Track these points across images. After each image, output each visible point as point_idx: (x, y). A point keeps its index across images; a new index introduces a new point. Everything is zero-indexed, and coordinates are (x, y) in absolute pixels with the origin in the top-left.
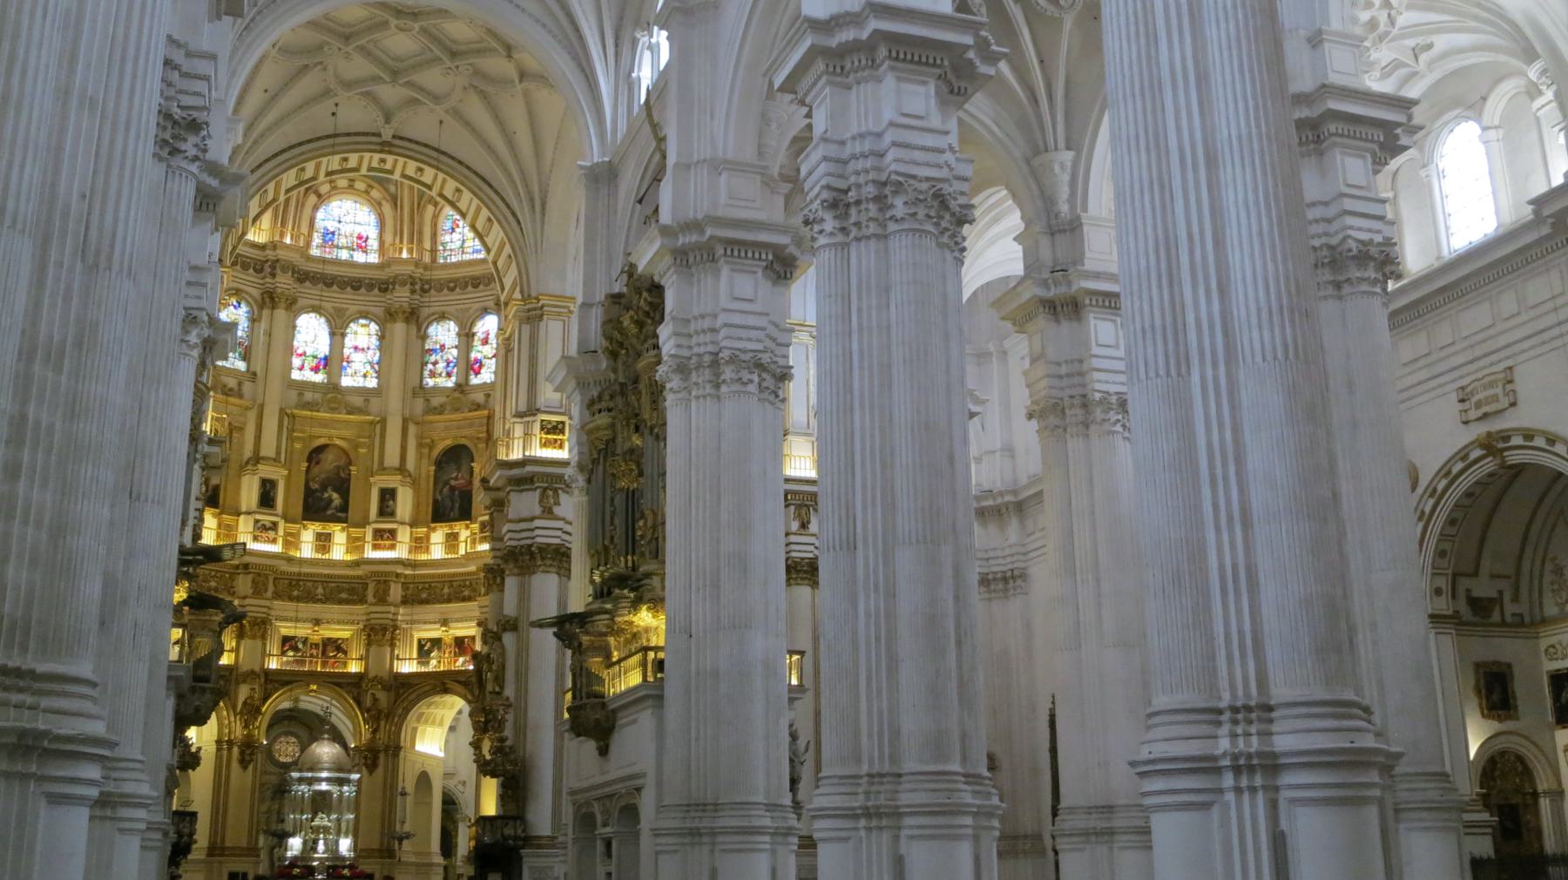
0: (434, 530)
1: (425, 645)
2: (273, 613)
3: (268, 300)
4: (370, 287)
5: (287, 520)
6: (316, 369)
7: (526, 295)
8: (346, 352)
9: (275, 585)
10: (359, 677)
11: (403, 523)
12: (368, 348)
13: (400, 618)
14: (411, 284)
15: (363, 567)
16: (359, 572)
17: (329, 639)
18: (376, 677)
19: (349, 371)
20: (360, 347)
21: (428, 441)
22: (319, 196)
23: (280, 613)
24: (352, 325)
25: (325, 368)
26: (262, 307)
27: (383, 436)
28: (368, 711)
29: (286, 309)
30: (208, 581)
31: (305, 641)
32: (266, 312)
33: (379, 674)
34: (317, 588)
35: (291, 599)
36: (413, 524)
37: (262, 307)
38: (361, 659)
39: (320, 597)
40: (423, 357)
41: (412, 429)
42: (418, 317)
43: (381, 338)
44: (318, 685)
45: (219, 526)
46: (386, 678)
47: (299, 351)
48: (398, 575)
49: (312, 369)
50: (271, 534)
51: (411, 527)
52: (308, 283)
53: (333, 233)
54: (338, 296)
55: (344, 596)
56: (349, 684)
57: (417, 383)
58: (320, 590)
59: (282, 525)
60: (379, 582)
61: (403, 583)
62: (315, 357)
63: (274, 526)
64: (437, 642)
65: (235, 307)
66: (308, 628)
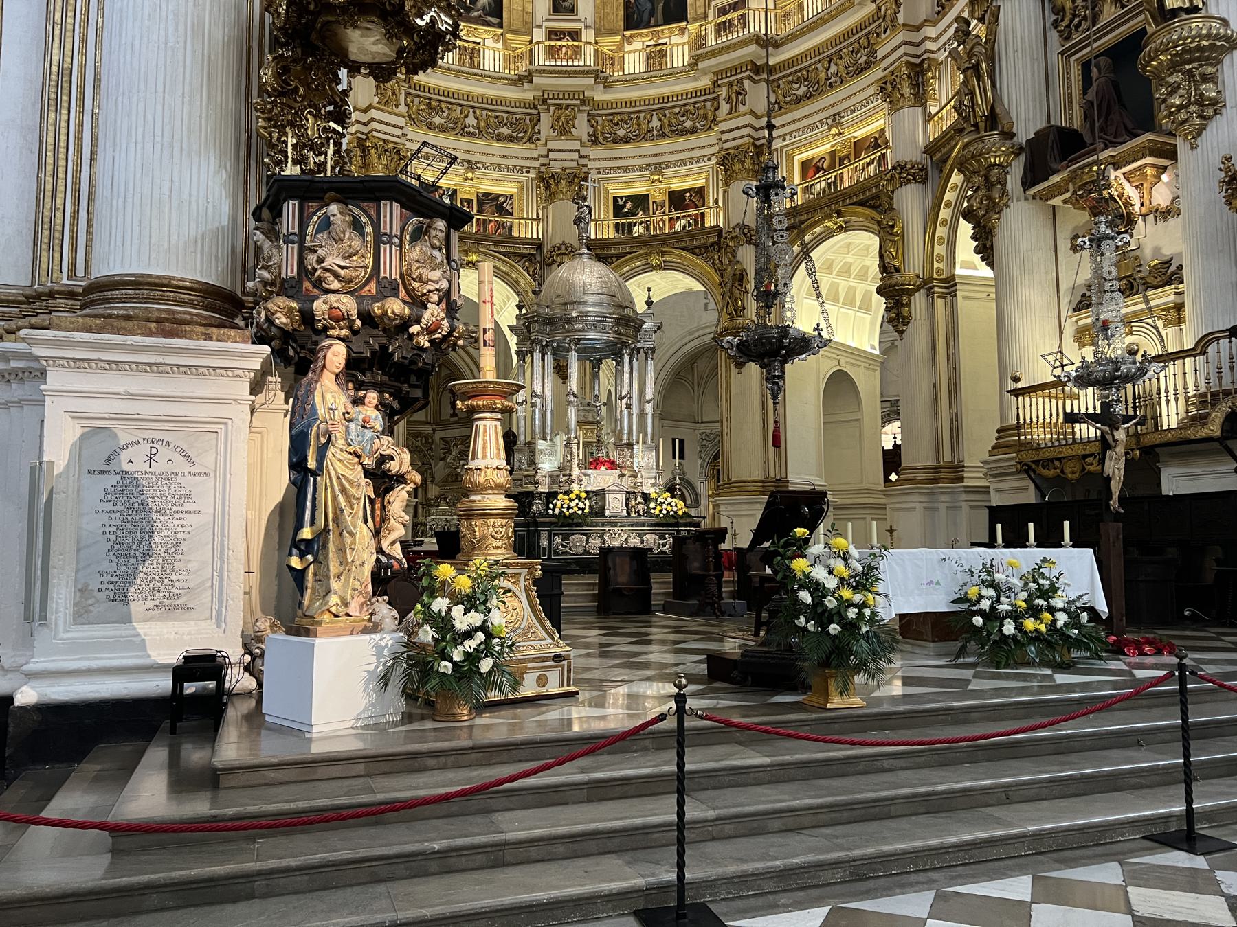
0: (630, 40)
1: (624, 206)
9: (407, 105)
10: (538, 245)
13: (591, 165)
16: (525, 94)
17: (486, 195)
18: (563, 243)
34: (466, 117)
38: (538, 219)
39: (471, 130)
55: (505, 131)
56: (522, 256)
58: (471, 120)
60: (559, 107)
61: (589, 115)
64: (641, 201)
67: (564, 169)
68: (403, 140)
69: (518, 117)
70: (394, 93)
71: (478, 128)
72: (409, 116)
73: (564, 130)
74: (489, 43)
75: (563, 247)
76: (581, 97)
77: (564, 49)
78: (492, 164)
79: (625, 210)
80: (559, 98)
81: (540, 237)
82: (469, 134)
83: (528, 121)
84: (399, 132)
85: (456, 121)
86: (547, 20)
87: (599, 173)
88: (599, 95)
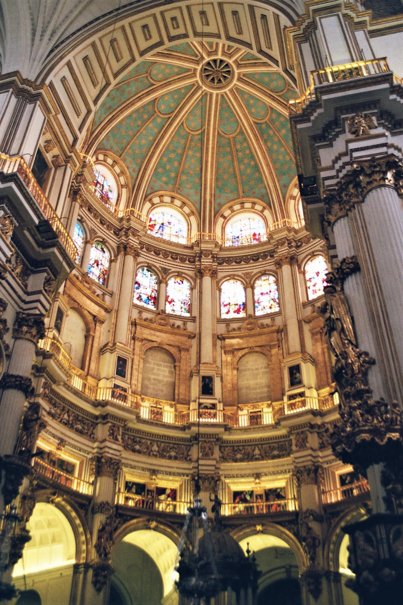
1: (346, 479)
2: (221, 473)
3: (198, 274)
4: (265, 257)
5: (225, 405)
6: (238, 311)
7: (295, 18)
8: (256, 298)
9: (222, 452)
10: (296, 514)
11: (310, 388)
12: (270, 292)
13: (320, 460)
14: (289, 244)
15: (283, 423)
16: (282, 432)
18: (308, 510)
19: (260, 308)
20: (265, 292)
21: (319, 329)
22: (225, 218)
23: (226, 472)
24: (257, 282)
25: (243, 310)
26: (195, 282)
27: (286, 335)
28: (304, 539)
29: (212, 277)
30: (169, 452)
31: (251, 493)
32: (198, 281)
33: (310, 508)
34: (254, 450)
35: (236, 461)
36: (318, 388)
37: (195, 282)
38: (294, 498)
39: (257, 456)
40: (306, 284)
41: (306, 328)
42: (297, 261)
43: (277, 282)
44: (263, 525)
45: (176, 410)
46: (317, 510)
47: (225, 303)
48: (312, 426)
49: (235, 312)
50: (212, 411)
51: (317, 390)
52: (225, 264)
53: (238, 237)
54: (246, 266)
55: (276, 453)
57: (306, 300)
58: (257, 452)
59: (220, 406)
60: (298, 434)
61: (318, 433)
62: (237, 305)
63: (214, 406)
65: (179, 284)
66: (250, 482)
67: (305, 467)
68: (217, 471)
69: (281, 443)
70: (210, 449)
71: (261, 455)
72: (223, 457)
73: (302, 445)
74: (266, 410)
75: (308, 512)
76: (308, 425)
77: (297, 403)
78: (269, 472)
79: (347, 482)
80: (297, 429)
81: (297, 509)
82: (257, 459)
83: (287, 444)
84: (213, 468)
85: (248, 454)
86: (288, 391)
87: (327, 464)
88: (318, 421)
